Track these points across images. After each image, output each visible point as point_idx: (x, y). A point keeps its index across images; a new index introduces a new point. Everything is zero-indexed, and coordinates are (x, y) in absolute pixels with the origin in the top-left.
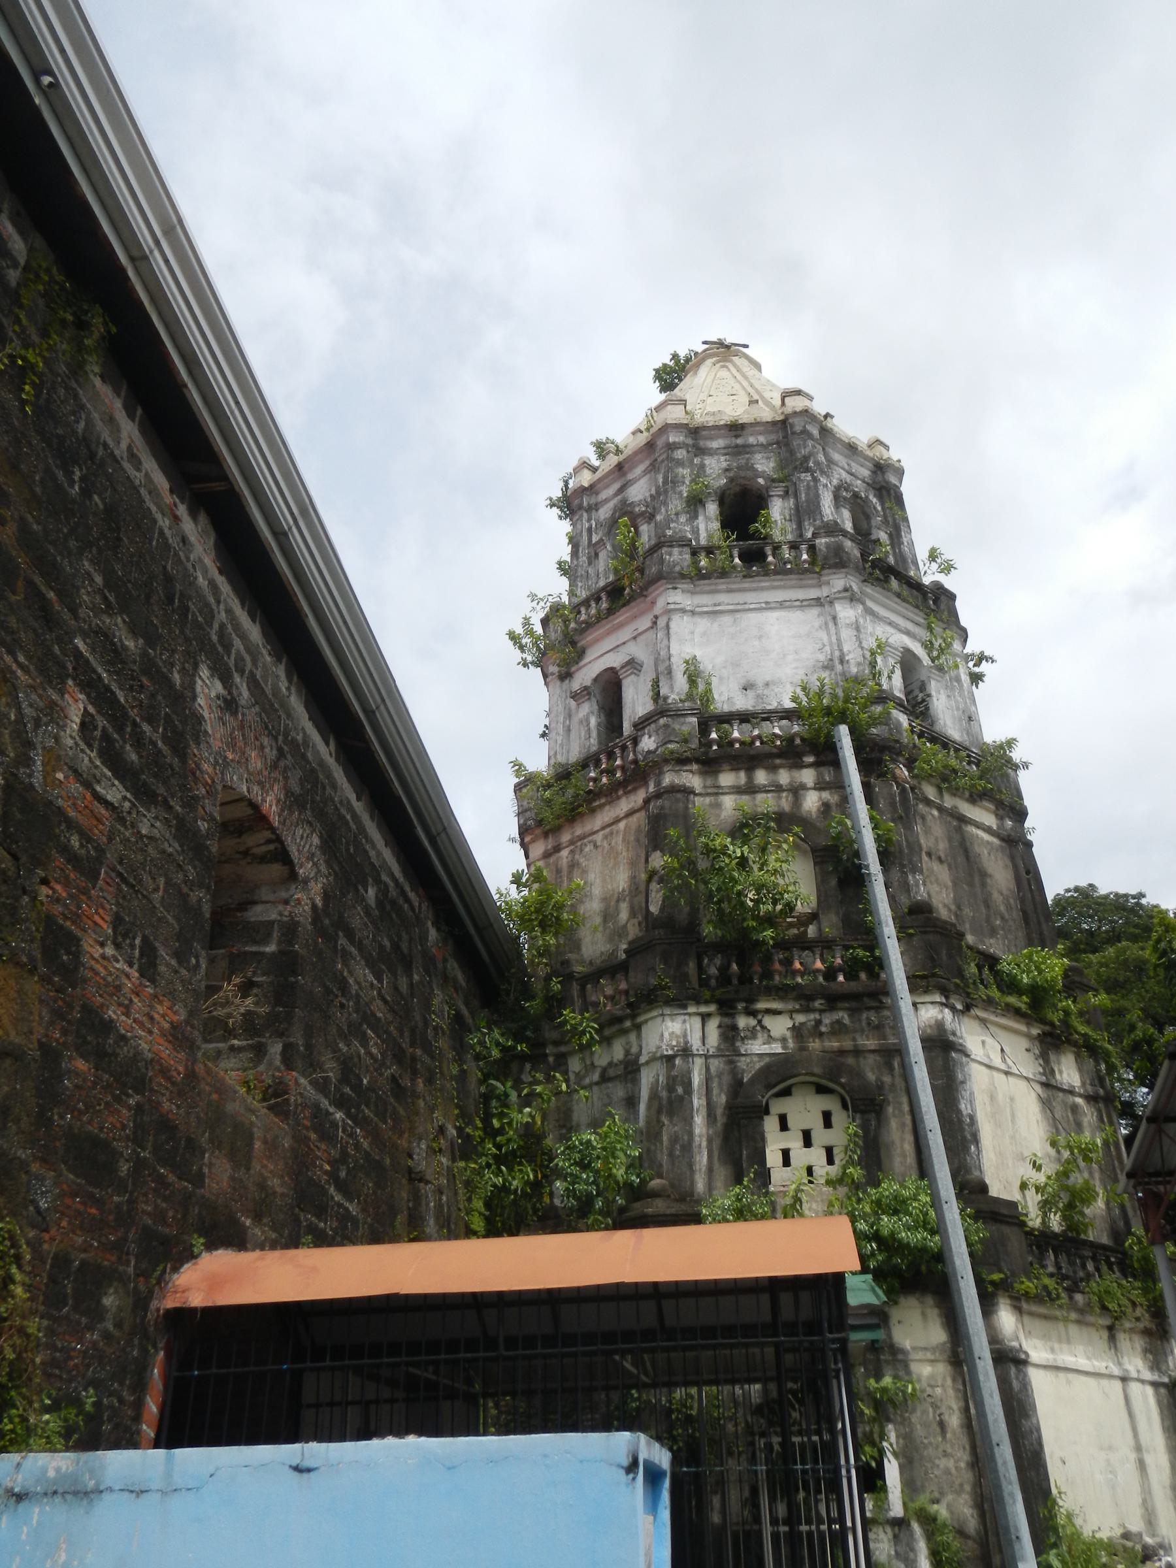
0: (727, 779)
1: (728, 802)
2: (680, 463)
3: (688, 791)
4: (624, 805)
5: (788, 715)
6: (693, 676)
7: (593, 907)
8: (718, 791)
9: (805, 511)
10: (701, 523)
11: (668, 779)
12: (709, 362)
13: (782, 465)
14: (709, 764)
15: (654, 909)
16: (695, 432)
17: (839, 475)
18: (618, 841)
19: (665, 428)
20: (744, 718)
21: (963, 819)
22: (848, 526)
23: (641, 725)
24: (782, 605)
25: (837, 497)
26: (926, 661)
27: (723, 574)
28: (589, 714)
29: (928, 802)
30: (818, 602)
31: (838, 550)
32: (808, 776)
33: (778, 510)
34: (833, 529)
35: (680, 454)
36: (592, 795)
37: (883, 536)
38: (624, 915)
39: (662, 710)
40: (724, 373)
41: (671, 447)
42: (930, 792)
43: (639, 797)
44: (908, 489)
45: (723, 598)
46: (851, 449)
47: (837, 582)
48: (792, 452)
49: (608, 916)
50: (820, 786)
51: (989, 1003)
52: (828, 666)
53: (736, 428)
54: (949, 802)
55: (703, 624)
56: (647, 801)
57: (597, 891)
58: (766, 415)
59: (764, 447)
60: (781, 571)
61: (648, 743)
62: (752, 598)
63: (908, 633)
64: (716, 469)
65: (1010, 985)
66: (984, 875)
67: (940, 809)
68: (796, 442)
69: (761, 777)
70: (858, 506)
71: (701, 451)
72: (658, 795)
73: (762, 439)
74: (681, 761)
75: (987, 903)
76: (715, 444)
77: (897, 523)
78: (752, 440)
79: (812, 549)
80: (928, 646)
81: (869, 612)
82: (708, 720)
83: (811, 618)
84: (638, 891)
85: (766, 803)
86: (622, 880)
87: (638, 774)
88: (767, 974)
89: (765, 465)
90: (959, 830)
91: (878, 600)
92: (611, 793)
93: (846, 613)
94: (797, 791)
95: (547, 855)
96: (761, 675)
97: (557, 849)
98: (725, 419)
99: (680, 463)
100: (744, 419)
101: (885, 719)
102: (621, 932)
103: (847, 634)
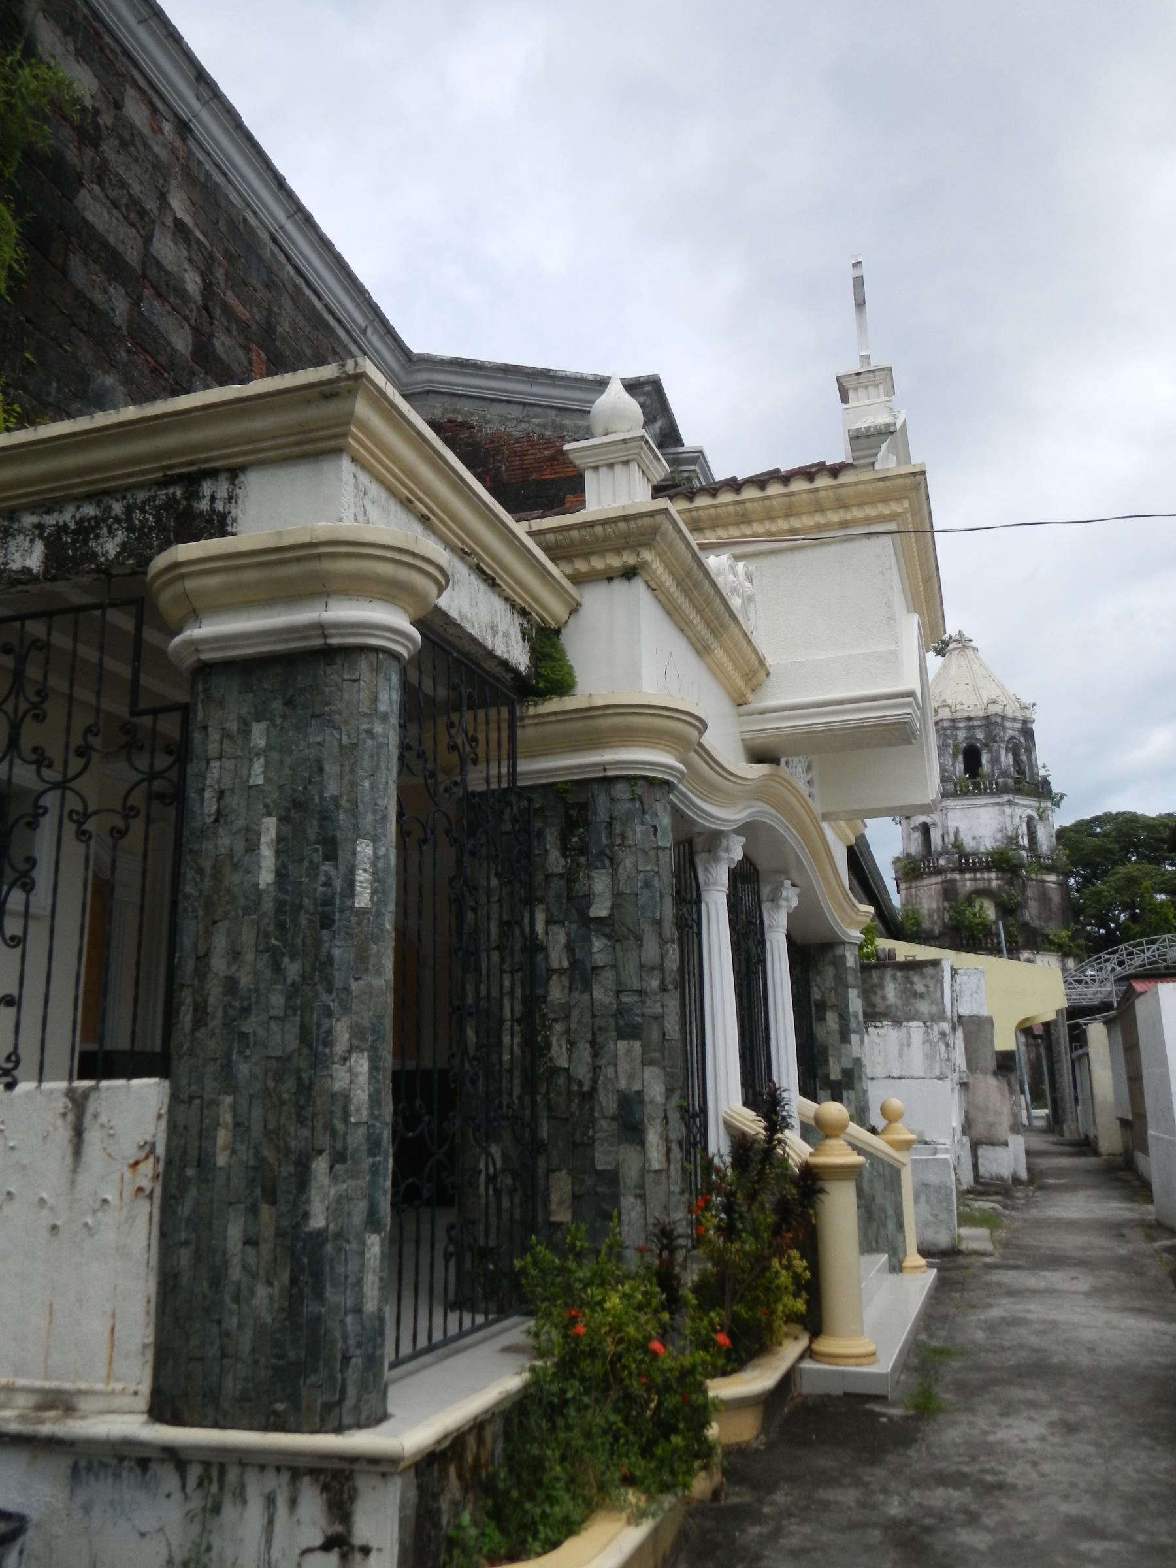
0: (968, 876)
1: (968, 883)
2: (948, 737)
3: (955, 881)
4: (934, 880)
5: (988, 854)
6: (956, 833)
7: (924, 912)
8: (964, 880)
9: (995, 761)
10: (957, 765)
11: (949, 876)
12: (956, 652)
13: (985, 738)
14: (962, 871)
15: (946, 920)
16: (953, 720)
17: (1010, 733)
18: (933, 892)
19: (942, 720)
20: (973, 854)
21: (1044, 881)
22: (1011, 762)
23: (940, 854)
24: (986, 805)
25: (1007, 749)
26: (1037, 817)
27: (965, 793)
28: (917, 835)
29: (1032, 880)
30: (998, 804)
31: (1006, 784)
32: (993, 875)
33: (985, 758)
34: (1004, 774)
35: (948, 732)
36: (924, 873)
37: (1024, 758)
38: (935, 917)
39: (944, 852)
40: (963, 661)
41: (945, 729)
42: (1033, 876)
43: (939, 879)
44: (1036, 728)
45: (966, 802)
46: (1014, 719)
47: (1006, 798)
48: (991, 732)
49: (930, 916)
50: (997, 879)
51: (1045, 950)
52: (1001, 831)
53: (969, 719)
54: (1040, 877)
55: (958, 813)
56: (942, 882)
57: (926, 906)
58: (981, 714)
59: (980, 726)
60: (986, 793)
61: (942, 862)
62: (976, 802)
63: (1030, 807)
64: (961, 735)
65: (1052, 943)
66: (1050, 900)
67: (1036, 880)
68: (992, 727)
69: (979, 875)
70: (1015, 750)
71: (955, 728)
72: (946, 882)
73: (979, 723)
74: (953, 870)
75: (1050, 910)
76: (961, 725)
77: (1030, 749)
78: (975, 723)
79: (997, 784)
80: (1038, 809)
81: (1017, 804)
82: (964, 855)
83: (994, 811)
84: (941, 911)
85: (980, 885)
86: (934, 906)
87: (939, 871)
88: (980, 943)
89: (980, 736)
90: (1043, 887)
91: (1020, 800)
92: (930, 875)
93: (1008, 810)
94: (990, 880)
95: (907, 889)
96: (979, 833)
97: (910, 888)
98: (966, 715)
99: (948, 737)
100: (973, 715)
101: (1021, 857)
102: (934, 923)
103: (1008, 819)
